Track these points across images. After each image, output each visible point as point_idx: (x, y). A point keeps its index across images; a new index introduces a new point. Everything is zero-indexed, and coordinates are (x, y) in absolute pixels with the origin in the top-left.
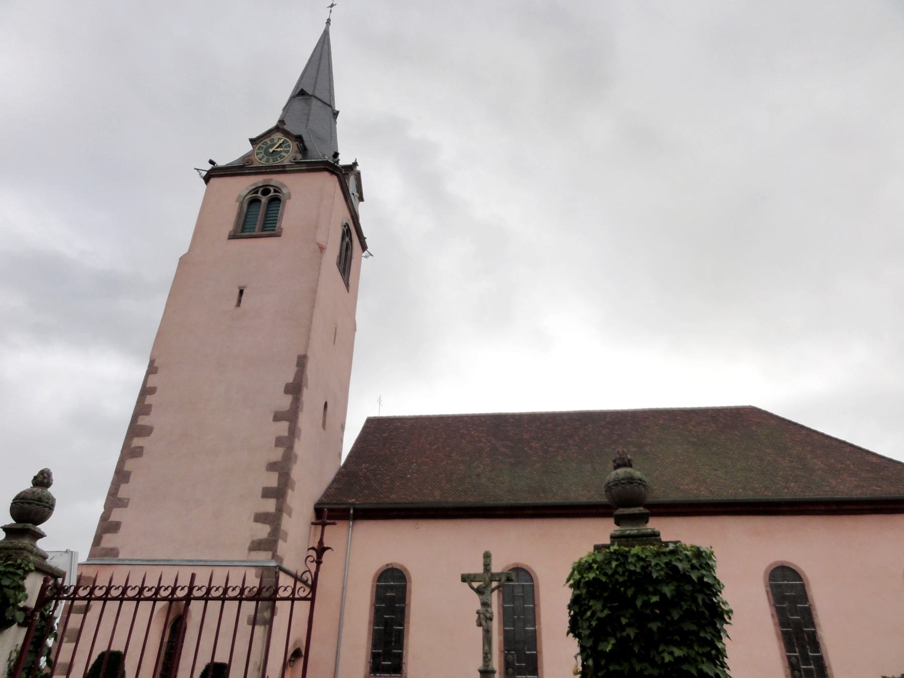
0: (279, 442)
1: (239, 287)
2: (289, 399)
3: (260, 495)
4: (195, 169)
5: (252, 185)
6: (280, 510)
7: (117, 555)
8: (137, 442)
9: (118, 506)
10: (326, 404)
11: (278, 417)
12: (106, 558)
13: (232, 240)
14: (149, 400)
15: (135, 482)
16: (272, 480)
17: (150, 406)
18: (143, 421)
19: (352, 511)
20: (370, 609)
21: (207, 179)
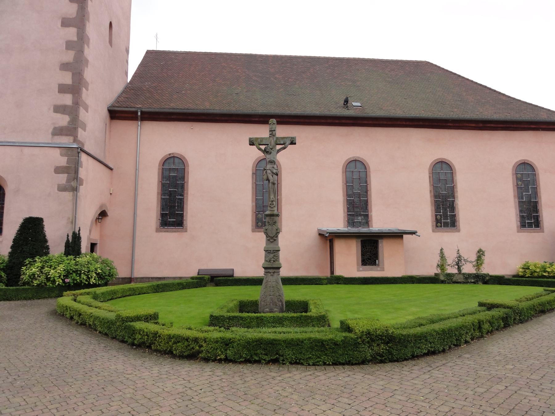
3: (57, 90)
16: (67, 78)
19: (139, 114)
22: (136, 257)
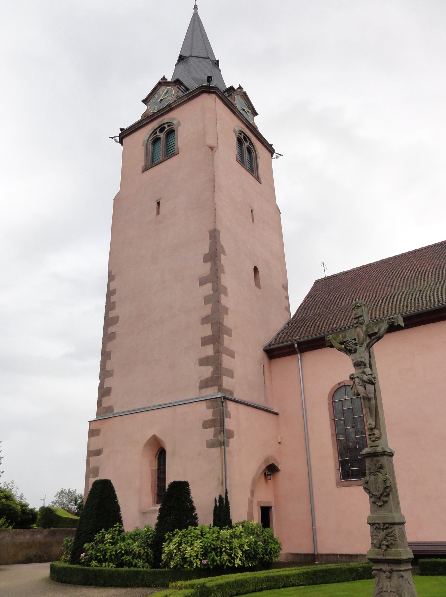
0: (207, 300)
1: (156, 201)
2: (208, 265)
3: (200, 344)
4: (110, 138)
5: (151, 130)
6: (218, 352)
7: (113, 411)
8: (111, 329)
9: (107, 377)
10: (256, 270)
11: (202, 282)
12: (108, 414)
13: (145, 172)
14: (113, 298)
15: (114, 357)
16: (207, 330)
17: (114, 303)
18: (112, 314)
19: (296, 346)
20: (331, 423)
21: (121, 142)
22: (318, 524)
